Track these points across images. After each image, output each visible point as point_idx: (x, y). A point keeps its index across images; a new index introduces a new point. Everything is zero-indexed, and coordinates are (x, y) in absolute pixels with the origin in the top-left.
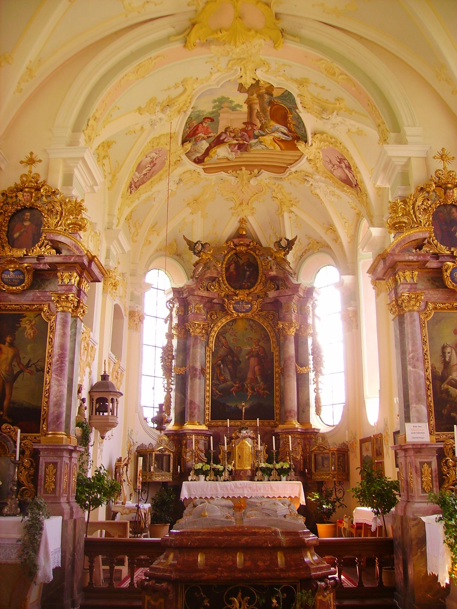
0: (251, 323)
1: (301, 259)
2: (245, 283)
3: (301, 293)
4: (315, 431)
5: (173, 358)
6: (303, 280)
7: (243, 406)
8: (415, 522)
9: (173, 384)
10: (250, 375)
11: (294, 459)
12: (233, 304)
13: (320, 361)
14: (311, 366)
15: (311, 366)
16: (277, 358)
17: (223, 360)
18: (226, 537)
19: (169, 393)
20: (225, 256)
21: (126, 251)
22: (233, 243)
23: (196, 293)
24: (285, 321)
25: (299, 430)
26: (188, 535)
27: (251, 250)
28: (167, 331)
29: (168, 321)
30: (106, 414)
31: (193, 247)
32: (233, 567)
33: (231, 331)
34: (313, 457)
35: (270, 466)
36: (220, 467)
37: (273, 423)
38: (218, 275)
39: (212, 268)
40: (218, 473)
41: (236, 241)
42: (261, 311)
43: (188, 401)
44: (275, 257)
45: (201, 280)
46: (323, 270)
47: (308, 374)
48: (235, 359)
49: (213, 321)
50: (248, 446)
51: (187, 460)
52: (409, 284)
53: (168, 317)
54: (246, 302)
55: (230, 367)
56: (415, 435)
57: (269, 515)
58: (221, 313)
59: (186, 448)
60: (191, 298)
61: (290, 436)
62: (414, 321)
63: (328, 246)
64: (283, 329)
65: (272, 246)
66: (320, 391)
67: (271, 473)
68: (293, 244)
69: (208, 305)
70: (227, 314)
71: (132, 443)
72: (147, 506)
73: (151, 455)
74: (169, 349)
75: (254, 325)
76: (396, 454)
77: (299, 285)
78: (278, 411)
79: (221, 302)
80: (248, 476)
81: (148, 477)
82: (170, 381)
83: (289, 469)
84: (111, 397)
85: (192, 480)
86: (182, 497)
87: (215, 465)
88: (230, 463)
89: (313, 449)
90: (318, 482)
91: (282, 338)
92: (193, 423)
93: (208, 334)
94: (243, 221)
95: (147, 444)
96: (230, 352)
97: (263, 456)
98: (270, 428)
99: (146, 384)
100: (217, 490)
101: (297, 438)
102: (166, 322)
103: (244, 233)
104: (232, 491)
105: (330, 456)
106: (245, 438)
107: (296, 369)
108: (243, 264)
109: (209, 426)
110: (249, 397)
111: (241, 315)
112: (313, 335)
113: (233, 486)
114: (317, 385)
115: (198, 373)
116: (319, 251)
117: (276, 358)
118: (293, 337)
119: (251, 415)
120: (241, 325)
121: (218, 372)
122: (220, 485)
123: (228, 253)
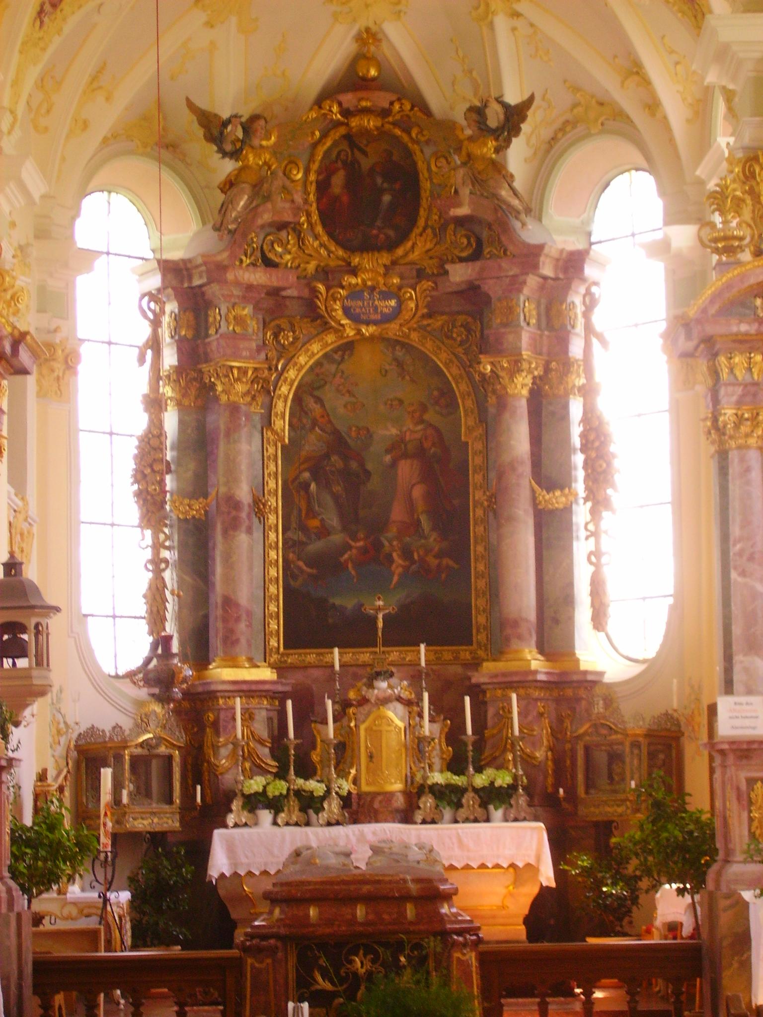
0: (400, 353)
3: (547, 270)
6: (551, 230)
7: (379, 609)
8: (727, 902)
9: (168, 548)
10: (398, 513)
11: (527, 761)
12: (342, 299)
13: (604, 472)
14: (580, 487)
15: (580, 487)
16: (478, 460)
17: (317, 468)
18: (344, 887)
19: (158, 573)
20: (315, 145)
21: (36, 197)
22: (340, 104)
24: (499, 352)
25: (541, 677)
26: (297, 885)
28: (145, 389)
30: (22, 663)
31: (216, 132)
32: (353, 920)
33: (337, 380)
34: (580, 754)
35: (458, 780)
36: (315, 786)
38: (296, 215)
40: (310, 804)
41: (348, 99)
43: (217, 597)
44: (469, 155)
47: (568, 510)
48: (354, 465)
49: (282, 351)
50: (394, 723)
52: (739, 385)
53: (147, 345)
55: (338, 488)
56: (738, 723)
57: (398, 861)
58: (306, 328)
59: (218, 734)
60: (214, 290)
61: (514, 696)
62: (748, 470)
65: (459, 115)
66: (604, 560)
67: (460, 800)
68: (523, 118)
69: (269, 303)
70: (326, 327)
71: (62, 726)
72: (125, 896)
73: (119, 758)
74: (154, 442)
76: (711, 759)
77: (540, 248)
78: (482, 619)
79: (306, 293)
80: (397, 811)
83: (513, 787)
84: (34, 621)
85: (236, 825)
87: (300, 781)
88: (342, 773)
89: (581, 731)
90: (596, 824)
91: (492, 400)
92: (234, 663)
94: (369, 37)
95: (107, 728)
96: (338, 443)
97: (438, 752)
98: (459, 669)
101: (537, 700)
102: (142, 360)
103: (373, 72)
105: (627, 749)
106: (385, 701)
108: (372, 170)
109: (281, 669)
110: (395, 578)
112: (588, 392)
113: (353, 839)
114: (597, 543)
115: (244, 515)
116: (604, 130)
117: (474, 461)
118: (524, 403)
119: (404, 630)
120: (367, 361)
121: (303, 505)
122: (317, 835)
123: (324, 136)
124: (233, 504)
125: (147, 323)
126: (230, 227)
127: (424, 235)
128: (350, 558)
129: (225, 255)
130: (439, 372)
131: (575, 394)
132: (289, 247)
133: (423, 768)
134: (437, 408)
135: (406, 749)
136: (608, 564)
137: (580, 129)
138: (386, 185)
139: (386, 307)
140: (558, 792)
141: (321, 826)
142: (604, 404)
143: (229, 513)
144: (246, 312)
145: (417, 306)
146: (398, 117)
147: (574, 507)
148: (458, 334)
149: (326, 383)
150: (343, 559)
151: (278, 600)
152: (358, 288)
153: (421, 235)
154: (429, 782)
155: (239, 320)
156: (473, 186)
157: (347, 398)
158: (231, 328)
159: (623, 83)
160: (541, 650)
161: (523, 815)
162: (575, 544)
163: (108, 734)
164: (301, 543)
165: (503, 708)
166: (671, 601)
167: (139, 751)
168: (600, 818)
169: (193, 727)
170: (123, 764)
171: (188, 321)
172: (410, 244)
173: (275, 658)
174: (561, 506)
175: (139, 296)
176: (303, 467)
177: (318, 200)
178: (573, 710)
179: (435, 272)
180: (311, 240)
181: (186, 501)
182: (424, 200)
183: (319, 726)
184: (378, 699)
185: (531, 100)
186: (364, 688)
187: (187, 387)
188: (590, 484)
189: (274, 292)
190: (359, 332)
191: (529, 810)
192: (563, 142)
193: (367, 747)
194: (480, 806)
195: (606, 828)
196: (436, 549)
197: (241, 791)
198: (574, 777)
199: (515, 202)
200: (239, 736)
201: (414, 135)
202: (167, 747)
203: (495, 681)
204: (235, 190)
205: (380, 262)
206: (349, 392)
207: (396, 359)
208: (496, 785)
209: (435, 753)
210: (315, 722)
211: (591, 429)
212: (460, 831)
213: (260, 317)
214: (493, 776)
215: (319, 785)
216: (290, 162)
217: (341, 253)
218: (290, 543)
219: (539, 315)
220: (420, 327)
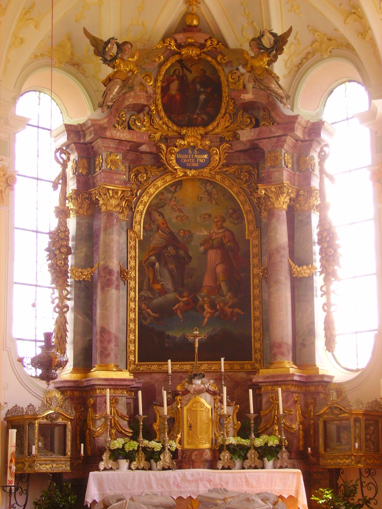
0: (209, 188)
1: (299, 70)
2: (198, 115)
3: (299, 133)
4: (326, 379)
5: (69, 252)
6: (302, 110)
7: (196, 336)
9: (69, 299)
10: (207, 281)
11: (288, 430)
13: (333, 255)
14: (317, 264)
15: (317, 264)
16: (256, 250)
19: (62, 314)
20: (161, 65)
22: (176, 41)
23: (108, 134)
25: (296, 378)
27: (208, 55)
28: (57, 204)
29: (60, 186)
31: (101, 49)
33: (172, 203)
34: (321, 426)
36: (155, 445)
37: (249, 367)
38: (148, 101)
39: (137, 88)
40: (152, 456)
41: (180, 37)
42: (226, 165)
43: (97, 329)
44: (252, 67)
45: (117, 110)
46: (339, 91)
47: (310, 278)
48: (182, 252)
49: (140, 185)
50: (205, 406)
51: (97, 434)
54: (199, 150)
58: (154, 171)
59: (95, 411)
60: (99, 143)
61: (280, 389)
63: (348, 46)
64: (267, 197)
65: (246, 47)
66: (332, 309)
67: (246, 454)
69: (132, 156)
73: (31, 425)
74: (62, 235)
75: (214, 191)
77: (296, 117)
78: (258, 345)
79: (154, 150)
80: (206, 461)
81: (27, 464)
82: (65, 293)
83: (279, 447)
85: (105, 469)
86: (89, 500)
87: (146, 442)
88: (172, 437)
89: (322, 412)
90: (330, 471)
93: (131, 208)
95: (25, 406)
96: (172, 239)
97: (232, 424)
99: (21, 298)
100: (151, 487)
102: (55, 187)
103: (195, 22)
104: (178, 486)
105: (352, 423)
106: (199, 392)
107: (291, 270)
108: (194, 80)
109: (135, 373)
110: (206, 320)
111: (191, 173)
112: (322, 208)
113: (179, 479)
114: (328, 299)
115: (114, 278)
116: (332, 55)
117: (253, 251)
118: (284, 213)
119: (210, 351)
120: (190, 192)
123: (166, 60)
124: (108, 271)
125: (59, 166)
126: (108, 104)
127: (225, 118)
128: (178, 308)
129: (105, 121)
130: (233, 199)
131: (314, 210)
132: (145, 123)
133: (223, 434)
134: (231, 220)
135: (213, 422)
136: (335, 311)
137: (317, 56)
138: (202, 89)
139: (202, 159)
140: (308, 450)
141: (159, 470)
142: (333, 216)
143: (105, 277)
144: (118, 157)
145: (220, 159)
146: (209, 49)
147: (315, 277)
148: (244, 176)
149: (165, 204)
150: (174, 308)
151: (135, 332)
152: (185, 147)
153: (223, 118)
154: (227, 443)
155: (114, 163)
156: (255, 82)
157: (178, 213)
158: (109, 167)
159: (345, 20)
160: (295, 361)
161: (285, 464)
162: (315, 299)
163: (25, 410)
164: (151, 298)
165: (272, 398)
166: (376, 332)
167: (45, 421)
168: (333, 467)
169: (81, 408)
170: (34, 429)
171: (84, 164)
172: (215, 123)
173: (133, 366)
174: (307, 275)
175: (54, 150)
176: (151, 253)
177: (162, 98)
178: (315, 399)
179: (231, 139)
180: (158, 120)
181: (80, 270)
182: (225, 98)
183: (158, 408)
184: (195, 390)
185: (290, 30)
186: (187, 384)
187: (82, 203)
188: (324, 262)
189: (135, 147)
190: (185, 174)
191: (289, 461)
192: (307, 64)
193: (188, 421)
194: (258, 458)
195: (336, 473)
196: (230, 303)
197: (109, 447)
198: (316, 440)
199: (280, 92)
200: (109, 413)
201: (219, 59)
202: (63, 419)
203: (267, 380)
204: (112, 83)
205: (199, 133)
206: (179, 209)
207: (207, 191)
208: (269, 445)
209: (230, 425)
210: (156, 405)
211: (324, 230)
212: (247, 474)
213: (127, 164)
214: (267, 439)
215: (158, 444)
216: (146, 75)
217: (175, 128)
218: (143, 298)
219: (293, 162)
220: (221, 172)
